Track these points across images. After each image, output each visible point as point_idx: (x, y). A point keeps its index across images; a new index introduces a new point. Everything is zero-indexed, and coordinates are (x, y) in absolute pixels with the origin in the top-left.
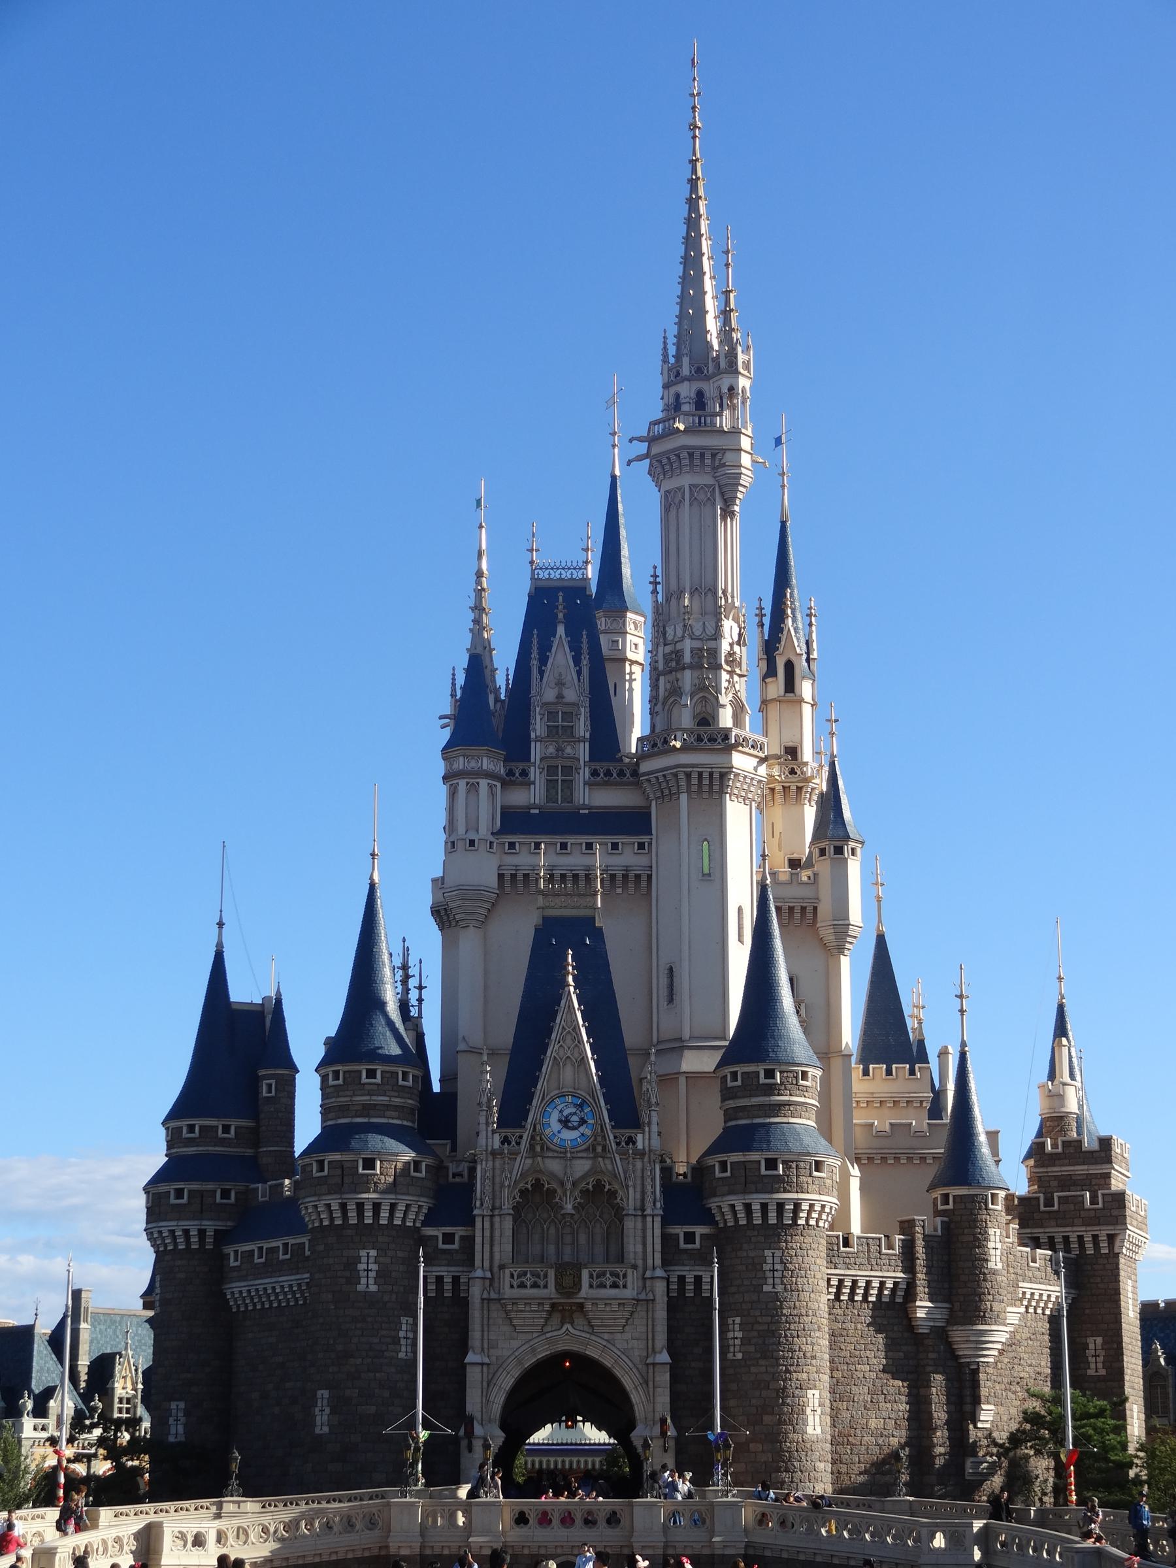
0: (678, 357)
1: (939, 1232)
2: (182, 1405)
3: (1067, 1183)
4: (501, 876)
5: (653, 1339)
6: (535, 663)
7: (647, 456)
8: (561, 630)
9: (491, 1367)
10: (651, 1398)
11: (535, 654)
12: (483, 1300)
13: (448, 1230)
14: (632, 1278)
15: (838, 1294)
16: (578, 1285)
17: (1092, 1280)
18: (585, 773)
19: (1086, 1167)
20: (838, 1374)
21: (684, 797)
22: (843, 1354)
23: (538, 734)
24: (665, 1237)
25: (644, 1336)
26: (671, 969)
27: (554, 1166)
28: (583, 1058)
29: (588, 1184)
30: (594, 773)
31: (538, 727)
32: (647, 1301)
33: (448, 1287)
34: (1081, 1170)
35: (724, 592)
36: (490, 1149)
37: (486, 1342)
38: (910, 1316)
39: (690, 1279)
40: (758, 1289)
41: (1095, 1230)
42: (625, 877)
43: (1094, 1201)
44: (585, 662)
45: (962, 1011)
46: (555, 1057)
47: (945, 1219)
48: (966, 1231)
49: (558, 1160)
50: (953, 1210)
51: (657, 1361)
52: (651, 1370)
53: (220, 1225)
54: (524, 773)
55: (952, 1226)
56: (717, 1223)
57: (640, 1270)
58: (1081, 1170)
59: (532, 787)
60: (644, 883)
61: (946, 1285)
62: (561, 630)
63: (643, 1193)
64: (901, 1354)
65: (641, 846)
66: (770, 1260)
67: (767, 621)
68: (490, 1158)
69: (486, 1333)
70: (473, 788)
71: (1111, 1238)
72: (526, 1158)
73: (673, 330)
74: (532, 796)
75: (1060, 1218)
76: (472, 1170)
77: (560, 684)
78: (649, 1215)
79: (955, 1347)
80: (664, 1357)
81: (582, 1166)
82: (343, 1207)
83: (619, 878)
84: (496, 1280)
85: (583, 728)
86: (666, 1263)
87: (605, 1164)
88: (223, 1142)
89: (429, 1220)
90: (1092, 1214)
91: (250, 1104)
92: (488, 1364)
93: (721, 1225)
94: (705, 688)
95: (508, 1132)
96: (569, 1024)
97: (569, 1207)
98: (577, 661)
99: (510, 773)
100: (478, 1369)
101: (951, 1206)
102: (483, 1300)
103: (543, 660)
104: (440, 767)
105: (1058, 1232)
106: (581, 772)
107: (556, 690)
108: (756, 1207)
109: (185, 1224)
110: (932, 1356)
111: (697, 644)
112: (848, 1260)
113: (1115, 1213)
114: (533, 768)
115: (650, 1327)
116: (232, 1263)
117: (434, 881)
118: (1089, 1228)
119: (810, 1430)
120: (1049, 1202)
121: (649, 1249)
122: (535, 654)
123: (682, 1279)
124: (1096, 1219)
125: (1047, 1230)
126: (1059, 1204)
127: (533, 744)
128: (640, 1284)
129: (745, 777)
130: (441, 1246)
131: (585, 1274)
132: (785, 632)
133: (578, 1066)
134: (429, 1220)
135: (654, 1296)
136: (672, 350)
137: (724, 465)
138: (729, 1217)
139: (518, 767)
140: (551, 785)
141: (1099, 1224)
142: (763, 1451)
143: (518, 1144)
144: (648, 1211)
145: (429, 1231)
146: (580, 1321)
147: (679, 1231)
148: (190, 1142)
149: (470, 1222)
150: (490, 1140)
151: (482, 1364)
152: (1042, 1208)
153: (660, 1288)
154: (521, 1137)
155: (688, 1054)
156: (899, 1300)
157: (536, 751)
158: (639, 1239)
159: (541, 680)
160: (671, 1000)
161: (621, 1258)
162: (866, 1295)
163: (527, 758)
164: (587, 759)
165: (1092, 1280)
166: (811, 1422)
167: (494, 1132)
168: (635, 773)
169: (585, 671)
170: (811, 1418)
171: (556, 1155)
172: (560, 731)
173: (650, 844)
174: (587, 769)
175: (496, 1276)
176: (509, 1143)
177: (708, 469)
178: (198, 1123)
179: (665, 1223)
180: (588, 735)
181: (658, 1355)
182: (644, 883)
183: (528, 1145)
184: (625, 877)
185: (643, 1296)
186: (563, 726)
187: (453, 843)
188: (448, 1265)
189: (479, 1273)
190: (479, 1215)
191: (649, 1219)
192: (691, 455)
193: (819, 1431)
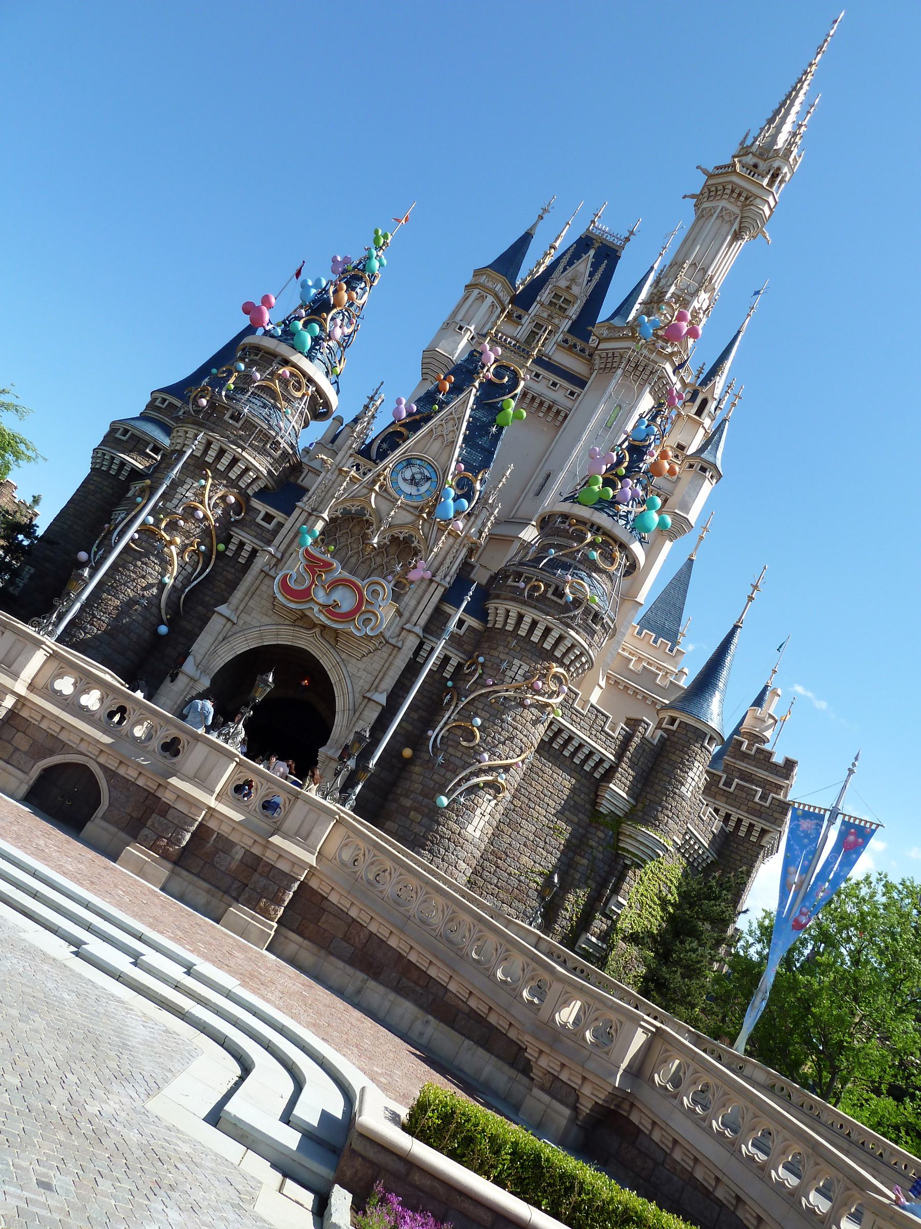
1: (655, 742)
2: (32, 571)
3: (746, 777)
5: (381, 680)
6: (561, 267)
8: (592, 252)
9: (236, 627)
10: (351, 726)
12: (262, 571)
13: (272, 511)
15: (552, 739)
17: (733, 856)
18: (559, 337)
19: (767, 773)
20: (516, 802)
21: (620, 371)
22: (532, 789)
23: (542, 299)
25: (376, 674)
26: (549, 476)
28: (453, 442)
29: (401, 533)
30: (566, 341)
31: (545, 296)
32: (395, 646)
33: (245, 554)
34: (762, 774)
35: (711, 279)
36: (341, 465)
37: (243, 604)
38: (599, 793)
41: (754, 820)
42: (550, 408)
43: (764, 797)
44: (597, 277)
45: (751, 599)
46: (432, 430)
47: (665, 735)
48: (677, 752)
49: (388, 503)
50: (675, 732)
51: (373, 698)
52: (364, 703)
54: (520, 317)
55: (668, 743)
56: (487, 622)
57: (404, 619)
58: (762, 774)
59: (520, 327)
60: (560, 418)
61: (639, 786)
62: (592, 252)
63: (441, 564)
64: (576, 819)
65: (572, 394)
66: (515, 669)
67: (702, 377)
68: (337, 472)
69: (247, 598)
70: (482, 298)
71: (764, 832)
72: (364, 487)
77: (573, 280)
78: (437, 582)
79: (621, 838)
80: (382, 699)
83: (546, 405)
84: (282, 563)
85: (574, 311)
90: (758, 807)
92: (234, 624)
93: (489, 625)
96: (458, 412)
98: (591, 275)
100: (224, 621)
101: (674, 728)
102: (262, 571)
103: (570, 263)
104: (468, 279)
106: (557, 335)
107: (568, 283)
110: (601, 835)
112: (574, 717)
113: (776, 815)
114: (527, 317)
115: (385, 668)
118: (750, 816)
119: (470, 829)
120: (728, 784)
121: (421, 608)
124: (758, 812)
125: (716, 802)
126: (735, 788)
127: (535, 303)
128: (397, 631)
129: (668, 383)
130: (259, 520)
132: (712, 383)
133: (446, 446)
135: (403, 645)
137: (752, 205)
138: (500, 619)
141: (760, 817)
142: (419, 823)
143: (365, 474)
144: (437, 579)
145: (256, 504)
148: (158, 409)
150: (345, 460)
151: (229, 620)
152: (721, 785)
154: (370, 470)
156: (597, 775)
157: (535, 309)
158: (417, 596)
159: (562, 273)
160: (538, 494)
162: (573, 754)
164: (566, 329)
165: (733, 856)
166: (475, 823)
167: (351, 455)
169: (594, 283)
170: (477, 819)
171: (389, 497)
172: (559, 305)
173: (579, 395)
174: (562, 335)
175: (284, 560)
176: (358, 469)
177: (739, 204)
180: (574, 317)
181: (377, 694)
182: (560, 418)
183: (371, 479)
184: (550, 408)
185: (393, 641)
186: (560, 306)
187: (448, 324)
188: (255, 537)
190: (300, 508)
191: (434, 585)
192: (733, 191)
193: (478, 834)
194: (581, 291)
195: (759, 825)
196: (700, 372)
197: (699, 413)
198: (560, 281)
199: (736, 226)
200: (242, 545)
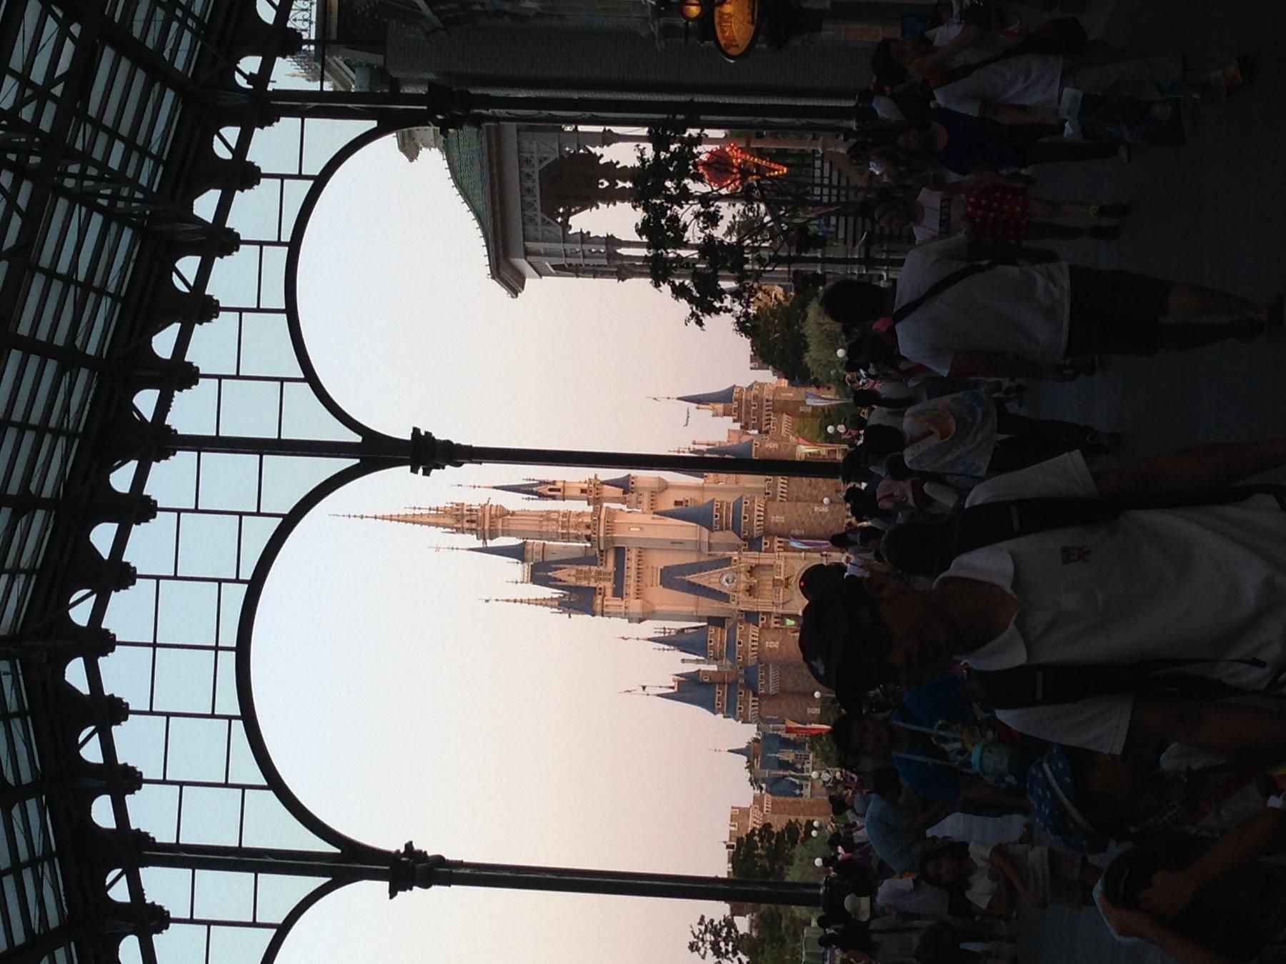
0: (452, 528)
3: (748, 413)
4: (637, 598)
7: (485, 539)
8: (550, 574)
11: (559, 583)
14: (778, 562)
16: (780, 580)
21: (614, 535)
24: (765, 552)
27: (742, 586)
30: (602, 565)
31: (585, 583)
39: (778, 544)
40: (783, 524)
43: (755, 406)
44: (562, 566)
53: (751, 694)
54: (600, 589)
62: (550, 574)
67: (531, 496)
70: (607, 606)
71: (767, 401)
74: (609, 586)
76: (742, 611)
77: (569, 575)
80: (803, 554)
81: (743, 578)
82: (753, 651)
85: (586, 568)
86: (773, 552)
87: (743, 569)
88: (723, 695)
89: (757, 626)
91: (711, 684)
94: (576, 525)
95: (731, 599)
97: (756, 581)
98: (561, 569)
99: (600, 594)
103: (560, 581)
108: (758, 523)
109: (750, 707)
111: (560, 528)
116: (763, 691)
117: (629, 622)
119: (826, 511)
122: (559, 583)
123: (779, 547)
131: (776, 577)
134: (757, 626)
136: (449, 530)
139: (598, 591)
140: (604, 580)
146: (789, 580)
147: (764, 547)
149: (758, 613)
153: (781, 554)
155: (702, 539)
157: (593, 584)
160: (681, 543)
161: (772, 566)
163: (595, 588)
168: (602, 551)
178: (717, 702)
179: (760, 551)
184: (640, 556)
189: (774, 610)
195: (765, 403)
196: (529, 499)
197: (559, 490)
198: (572, 581)
199: (509, 517)
200: (776, 623)
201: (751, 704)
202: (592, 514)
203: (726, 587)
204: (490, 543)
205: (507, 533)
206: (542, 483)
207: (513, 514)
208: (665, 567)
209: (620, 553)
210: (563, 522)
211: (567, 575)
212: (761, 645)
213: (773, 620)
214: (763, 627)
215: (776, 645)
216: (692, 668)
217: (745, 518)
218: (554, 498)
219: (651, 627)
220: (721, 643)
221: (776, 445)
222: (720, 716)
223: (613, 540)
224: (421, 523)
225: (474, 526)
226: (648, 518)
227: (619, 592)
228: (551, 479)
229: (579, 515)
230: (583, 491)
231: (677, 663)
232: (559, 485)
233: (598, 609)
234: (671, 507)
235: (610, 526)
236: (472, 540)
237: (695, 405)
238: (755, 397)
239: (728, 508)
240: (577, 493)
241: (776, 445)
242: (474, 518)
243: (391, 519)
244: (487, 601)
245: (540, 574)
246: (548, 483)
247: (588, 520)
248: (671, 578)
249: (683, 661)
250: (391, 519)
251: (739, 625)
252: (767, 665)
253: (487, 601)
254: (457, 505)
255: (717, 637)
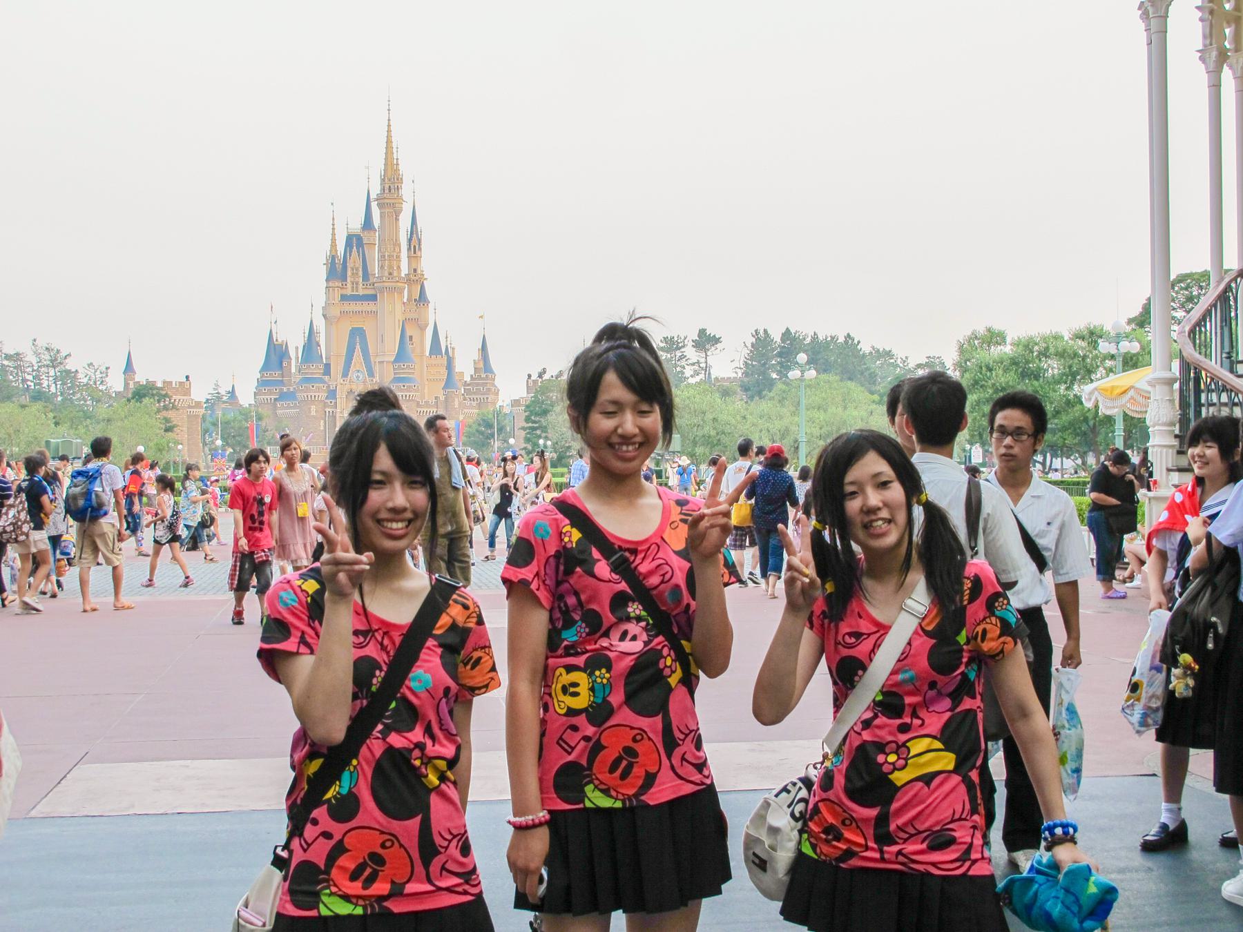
3: (478, 384)
7: (377, 200)
31: (349, 273)
73: (383, 168)
74: (349, 292)
75: (475, 393)
85: (361, 273)
98: (359, 255)
103: (350, 256)
105: (475, 397)
139: (344, 283)
163: (346, 280)
194: (359, 264)
197: (415, 252)
198: (350, 265)
201: (269, 397)
202: (400, 277)
203: (352, 374)
204: (374, 205)
205: (382, 216)
206: (420, 241)
207: (397, 219)
208: (364, 331)
209: (373, 298)
210: (393, 256)
211: (355, 261)
212: (313, 402)
213: (331, 410)
214: (325, 403)
215: (313, 413)
216: (292, 353)
217: (404, 386)
218: (409, 249)
219: (320, 324)
220: (312, 374)
221: (456, 406)
222: (259, 376)
223: (382, 292)
224: (386, 154)
225: (387, 191)
226: (399, 316)
227: (344, 298)
228: (422, 247)
229: (399, 267)
230: (415, 270)
231: (295, 343)
232: (418, 253)
233: (331, 284)
234: (408, 333)
235: (392, 290)
236: (376, 191)
237: (480, 347)
238: (489, 390)
239: (410, 373)
240: (414, 266)
241: (456, 406)
242: (393, 191)
243: (389, 131)
244: (332, 204)
245: (354, 241)
246: (420, 245)
247: (395, 274)
248: (357, 334)
249: (297, 348)
250: (389, 131)
251: (326, 385)
252: (298, 407)
253: (332, 204)
254: (402, 179)
255: (316, 370)
